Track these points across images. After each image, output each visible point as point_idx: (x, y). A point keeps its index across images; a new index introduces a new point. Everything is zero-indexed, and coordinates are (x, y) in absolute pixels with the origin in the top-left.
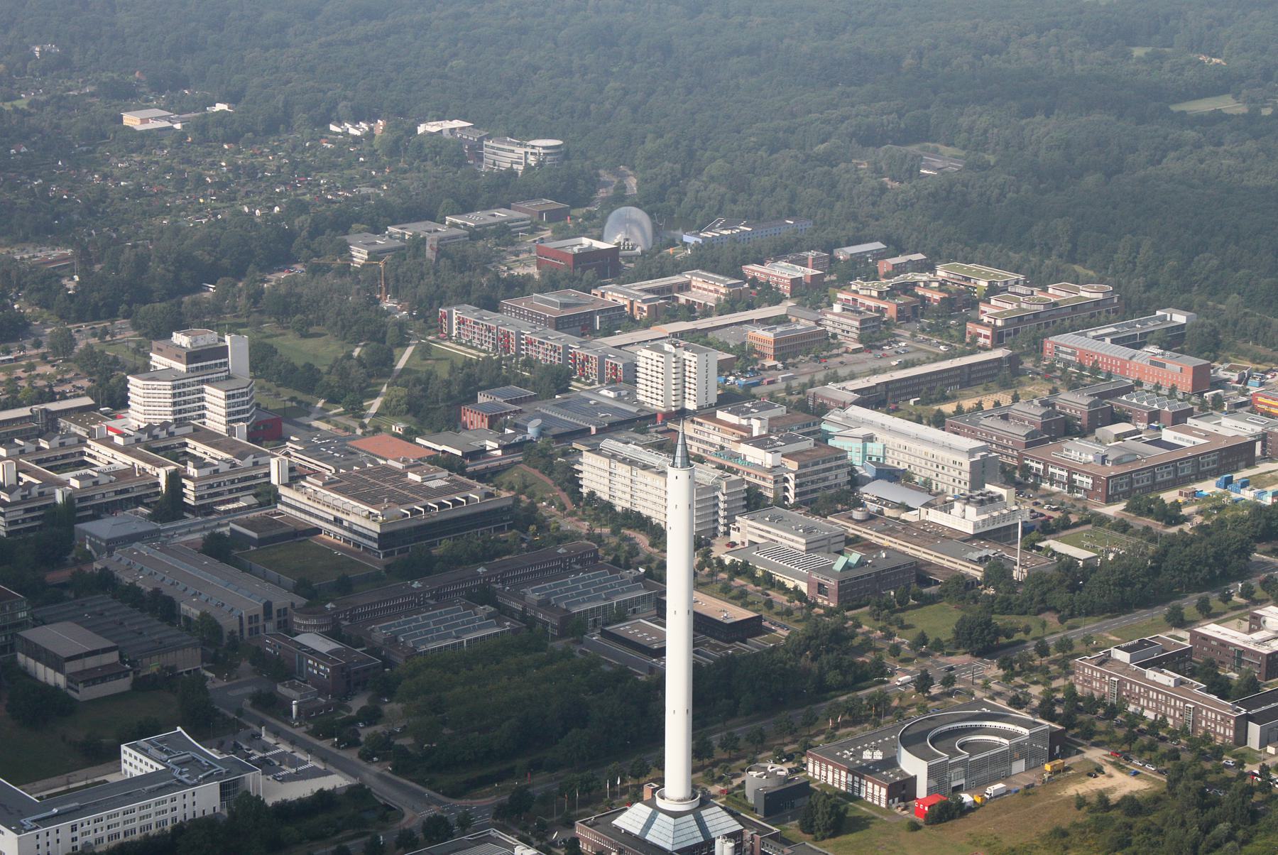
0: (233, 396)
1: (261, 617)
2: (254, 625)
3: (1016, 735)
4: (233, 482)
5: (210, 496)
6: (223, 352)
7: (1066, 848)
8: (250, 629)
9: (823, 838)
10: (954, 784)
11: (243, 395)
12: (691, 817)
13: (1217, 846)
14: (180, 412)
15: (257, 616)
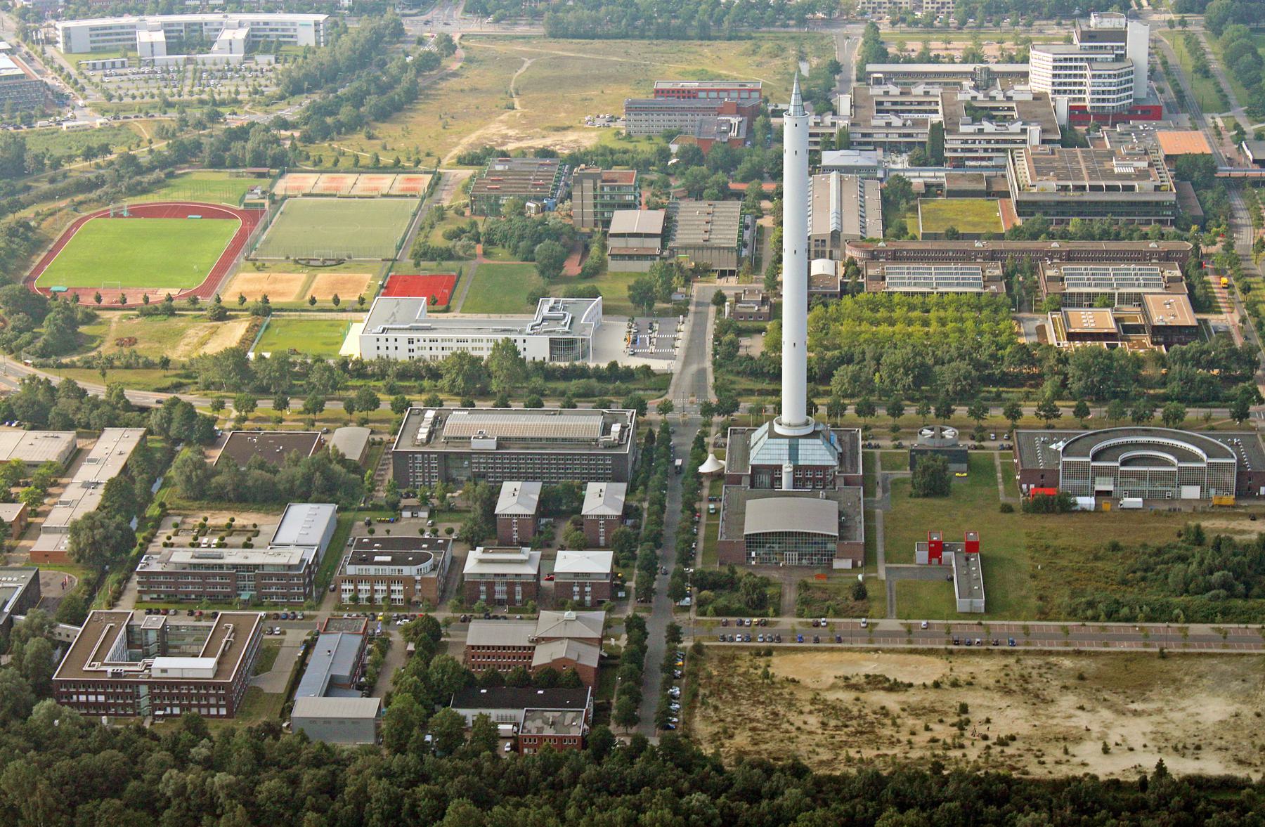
0: (1100, 76)
1: (828, 243)
2: (820, 249)
3: (1196, 458)
4: (989, 142)
5: (963, 150)
6: (1121, 35)
7: (1097, 558)
8: (816, 252)
9: (918, 496)
10: (1098, 488)
11: (1110, 76)
12: (787, 441)
13: (1208, 588)
14: (1060, 84)
15: (824, 241)
